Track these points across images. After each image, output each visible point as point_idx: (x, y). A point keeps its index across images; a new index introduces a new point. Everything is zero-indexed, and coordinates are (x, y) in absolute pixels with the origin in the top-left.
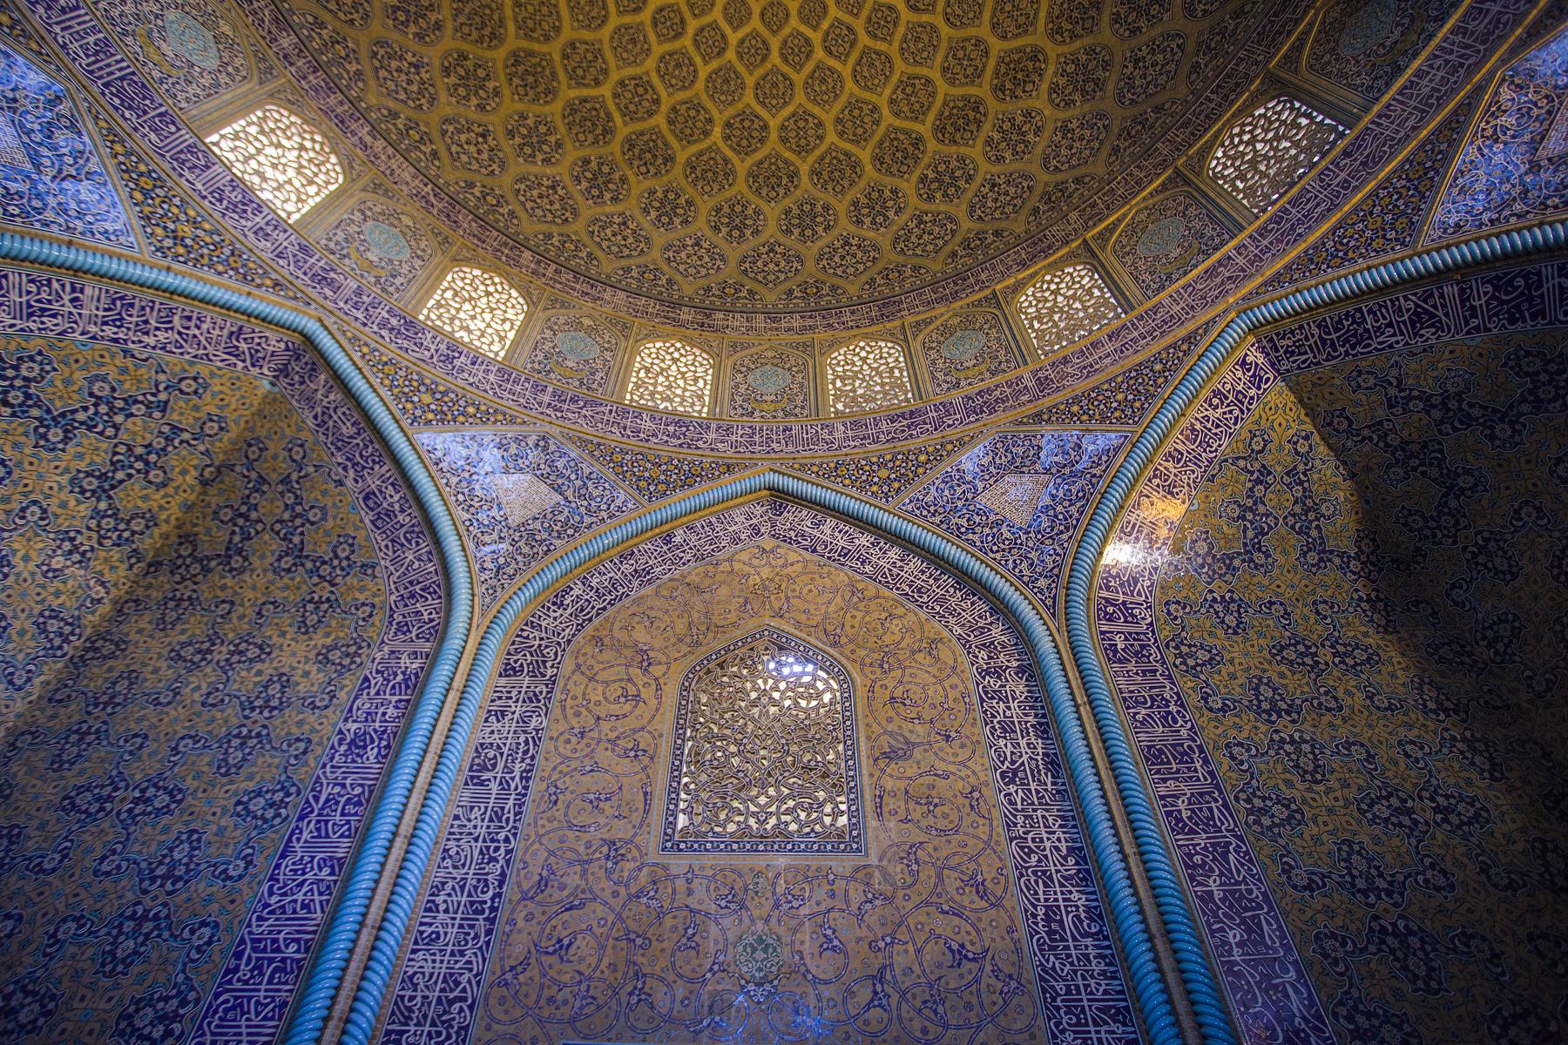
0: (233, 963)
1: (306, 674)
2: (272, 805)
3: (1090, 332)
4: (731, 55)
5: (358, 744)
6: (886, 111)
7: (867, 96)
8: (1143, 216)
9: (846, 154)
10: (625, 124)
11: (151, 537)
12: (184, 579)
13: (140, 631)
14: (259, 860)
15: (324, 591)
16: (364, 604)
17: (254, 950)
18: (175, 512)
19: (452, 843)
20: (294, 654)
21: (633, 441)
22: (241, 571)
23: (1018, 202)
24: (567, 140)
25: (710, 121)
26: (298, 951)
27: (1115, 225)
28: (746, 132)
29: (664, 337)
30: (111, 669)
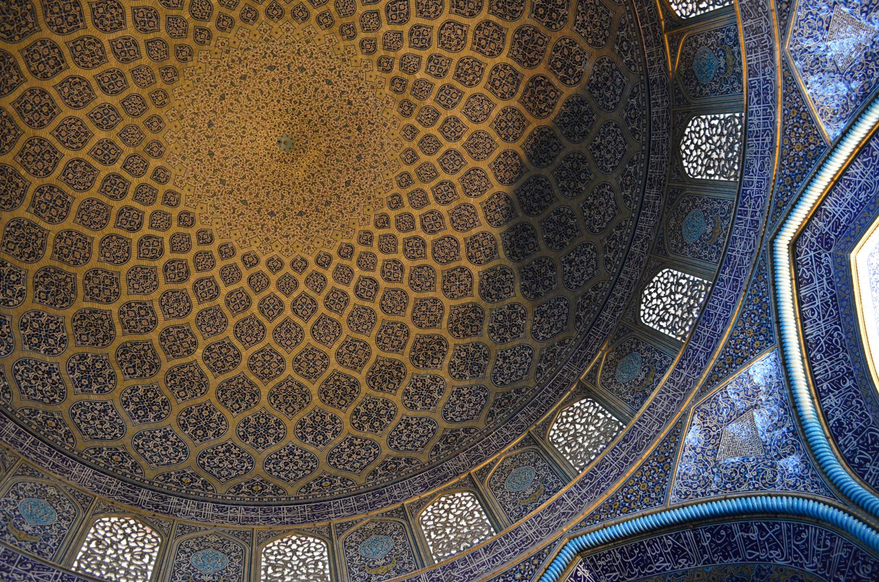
3: (472, 544)
4: (220, 301)
6: (333, 359)
7: (320, 346)
8: (509, 462)
9: (300, 385)
10: (124, 334)
23: (425, 439)
24: (71, 338)
25: (195, 344)
27: (490, 466)
28: (222, 357)
29: (120, 514)
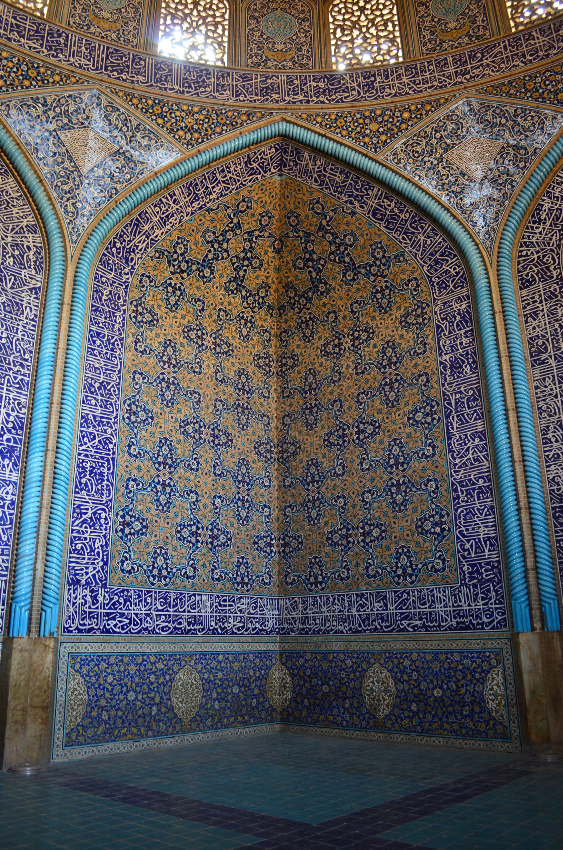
0: (455, 495)
1: (401, 337)
2: (427, 414)
5: (456, 366)
11: (271, 294)
12: (301, 310)
13: (298, 346)
14: (438, 444)
15: (381, 283)
16: (409, 281)
17: (462, 486)
18: (273, 275)
19: (541, 404)
20: (387, 328)
21: (536, 63)
22: (328, 291)
26: (485, 482)
30: (299, 372)
